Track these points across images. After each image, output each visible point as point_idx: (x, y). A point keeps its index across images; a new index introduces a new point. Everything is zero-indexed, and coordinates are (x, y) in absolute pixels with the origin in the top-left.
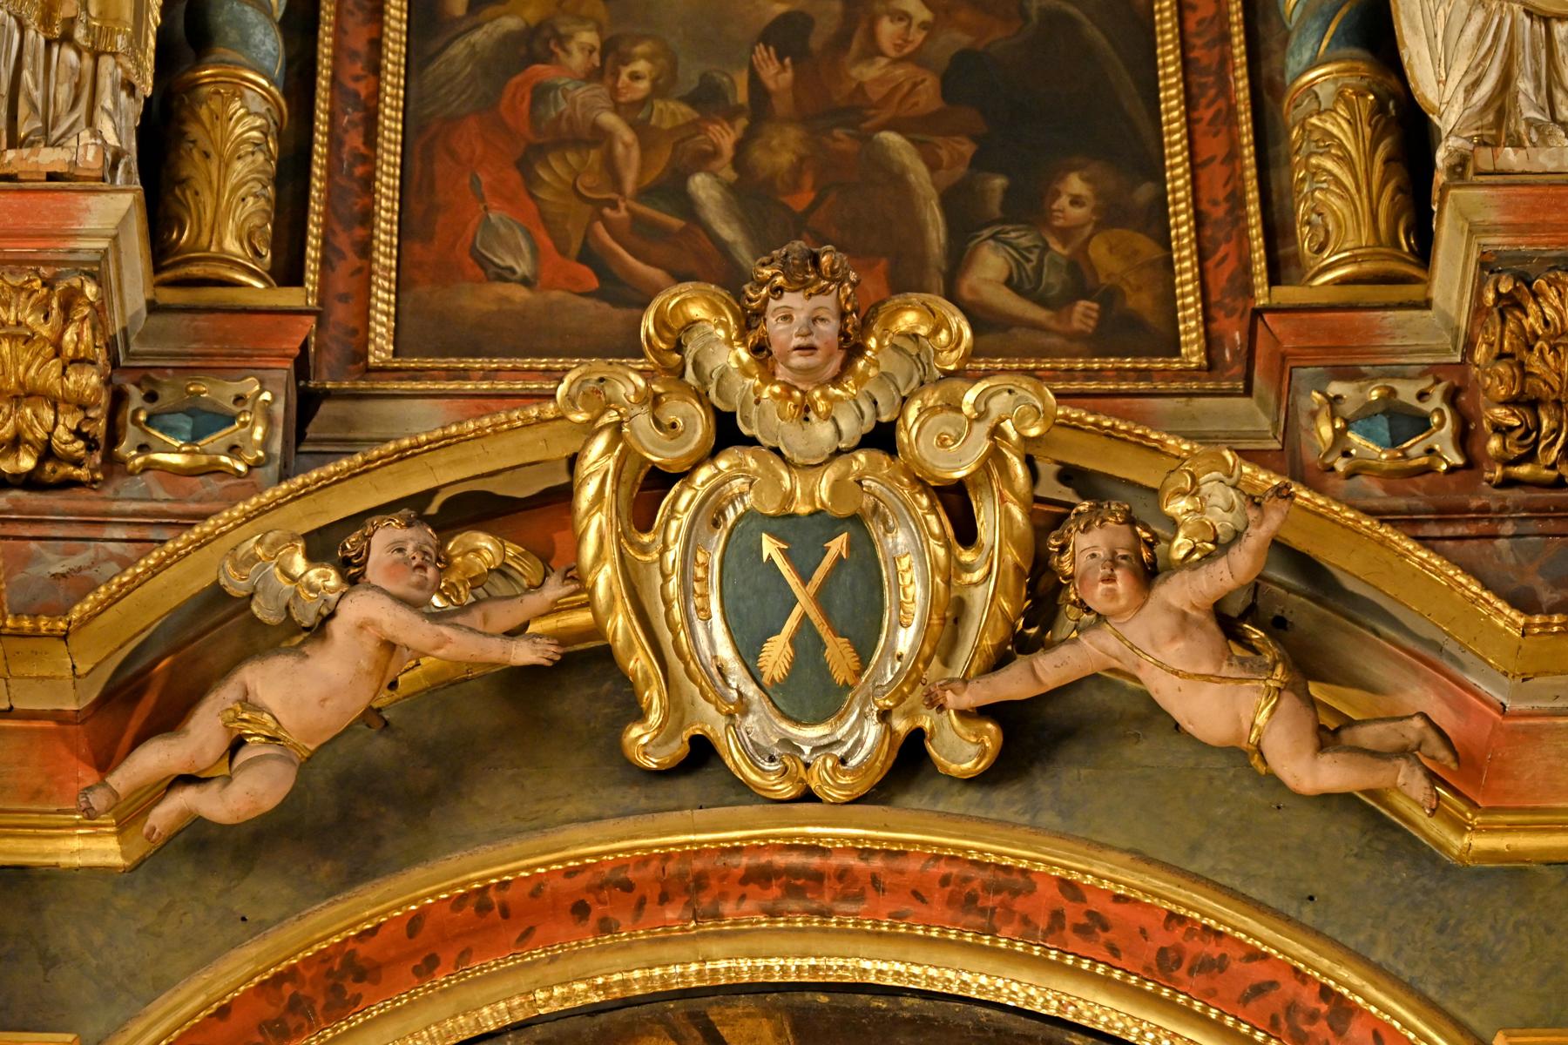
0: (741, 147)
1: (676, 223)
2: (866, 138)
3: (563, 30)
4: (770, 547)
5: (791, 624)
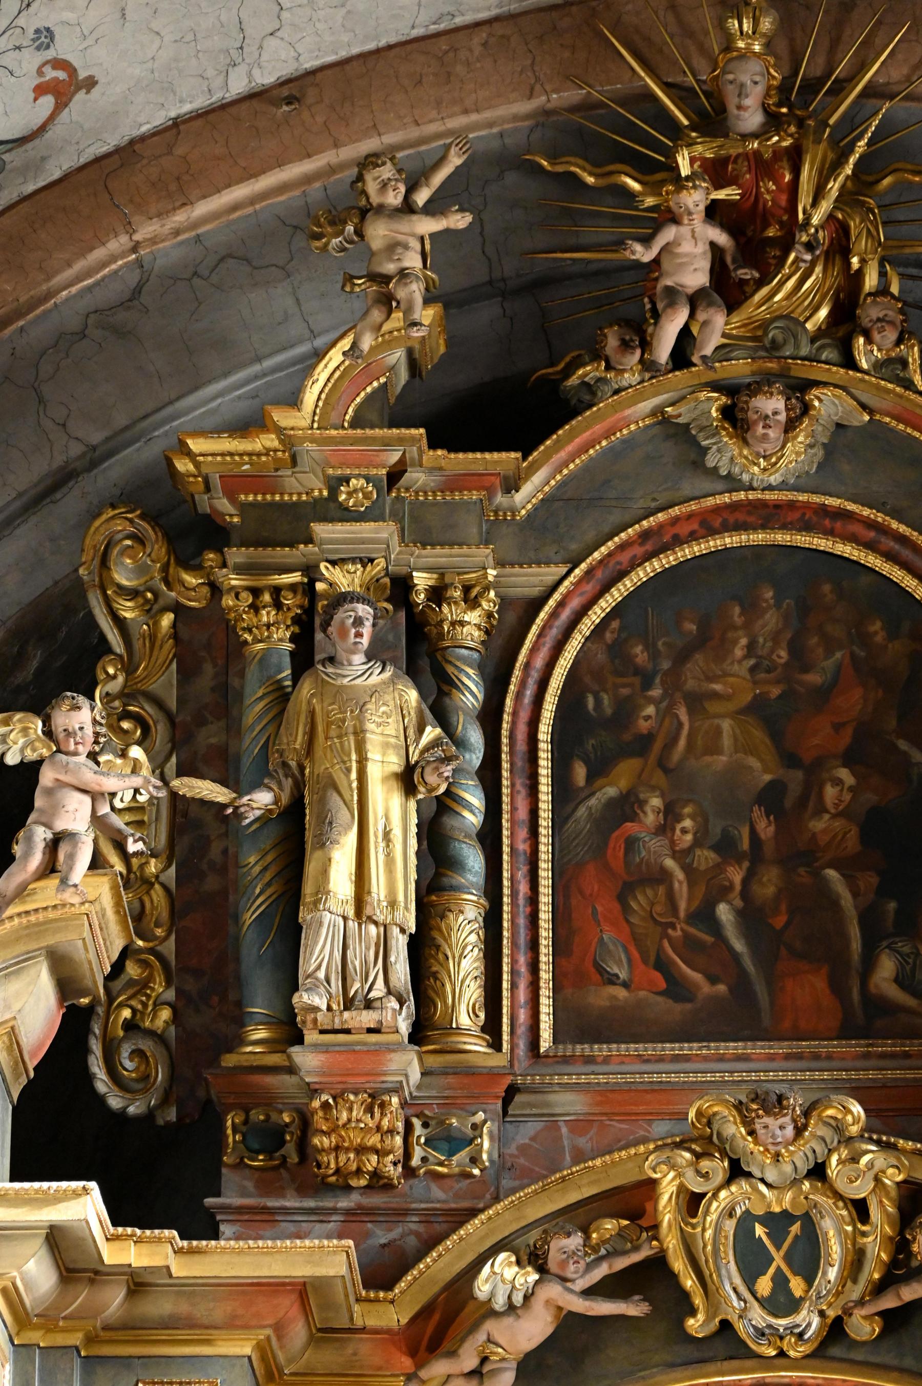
0: (745, 882)
1: (709, 939)
2: (817, 874)
3: (642, 796)
4: (759, 1231)
5: (772, 1271)
